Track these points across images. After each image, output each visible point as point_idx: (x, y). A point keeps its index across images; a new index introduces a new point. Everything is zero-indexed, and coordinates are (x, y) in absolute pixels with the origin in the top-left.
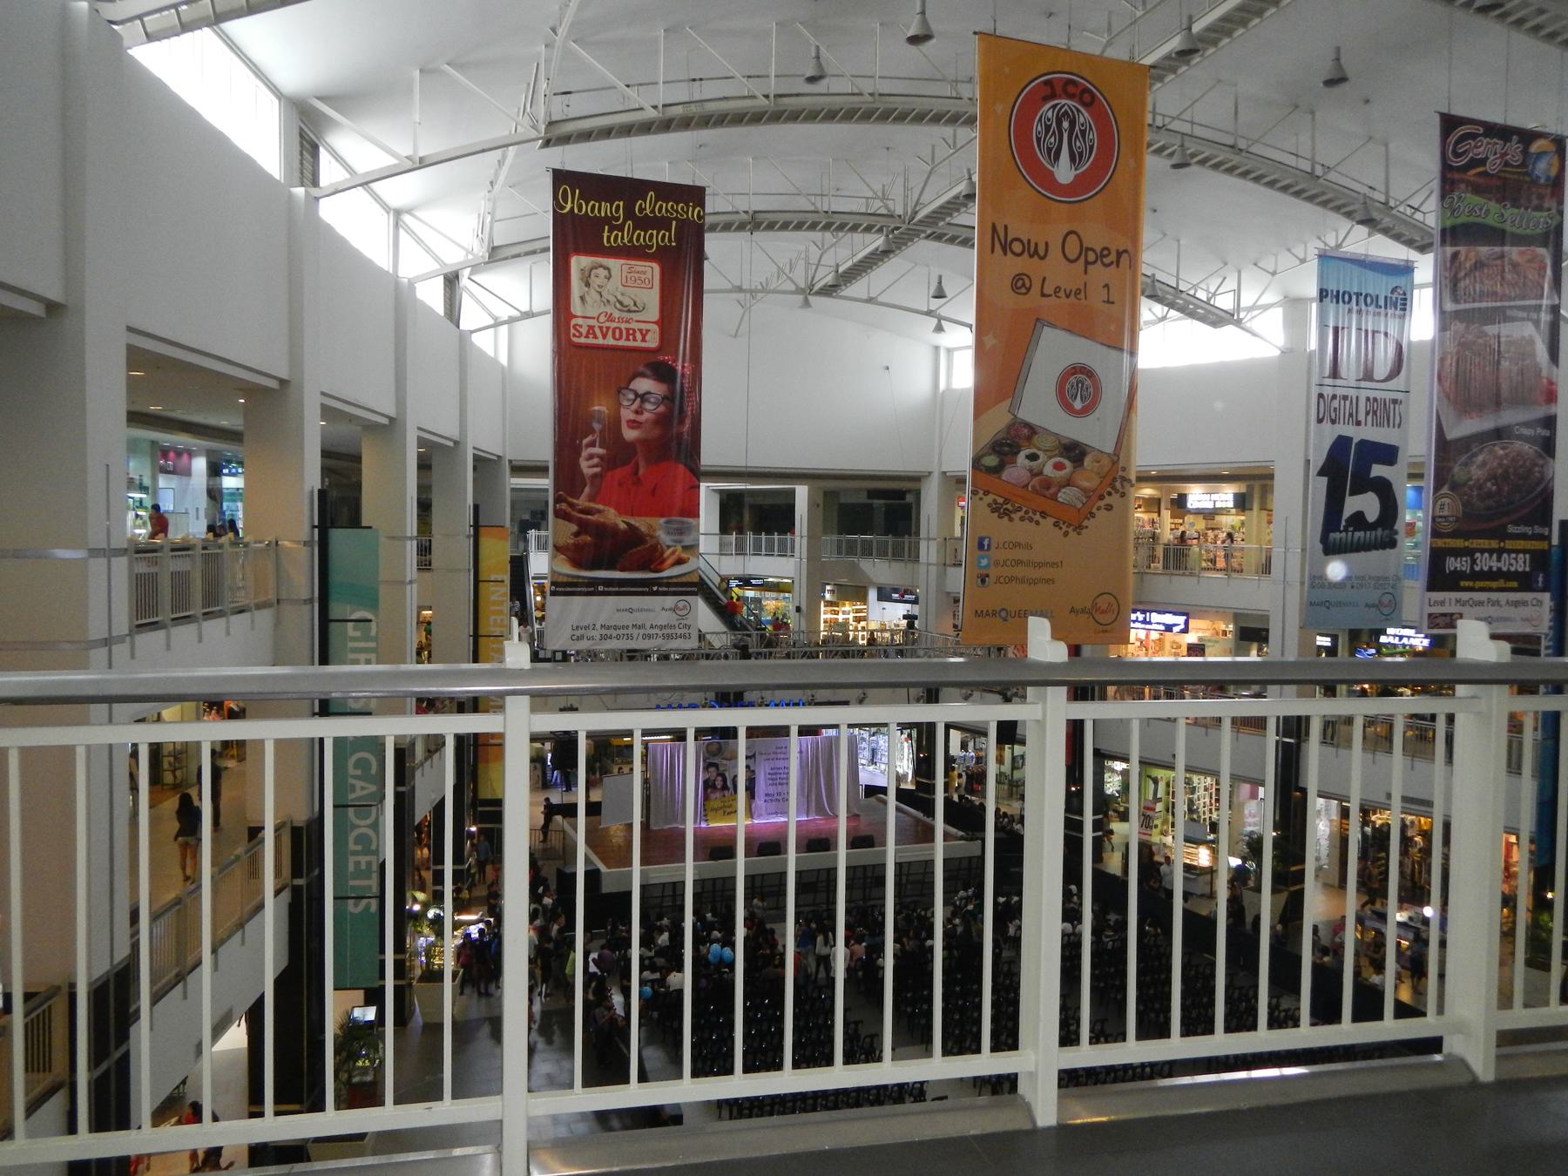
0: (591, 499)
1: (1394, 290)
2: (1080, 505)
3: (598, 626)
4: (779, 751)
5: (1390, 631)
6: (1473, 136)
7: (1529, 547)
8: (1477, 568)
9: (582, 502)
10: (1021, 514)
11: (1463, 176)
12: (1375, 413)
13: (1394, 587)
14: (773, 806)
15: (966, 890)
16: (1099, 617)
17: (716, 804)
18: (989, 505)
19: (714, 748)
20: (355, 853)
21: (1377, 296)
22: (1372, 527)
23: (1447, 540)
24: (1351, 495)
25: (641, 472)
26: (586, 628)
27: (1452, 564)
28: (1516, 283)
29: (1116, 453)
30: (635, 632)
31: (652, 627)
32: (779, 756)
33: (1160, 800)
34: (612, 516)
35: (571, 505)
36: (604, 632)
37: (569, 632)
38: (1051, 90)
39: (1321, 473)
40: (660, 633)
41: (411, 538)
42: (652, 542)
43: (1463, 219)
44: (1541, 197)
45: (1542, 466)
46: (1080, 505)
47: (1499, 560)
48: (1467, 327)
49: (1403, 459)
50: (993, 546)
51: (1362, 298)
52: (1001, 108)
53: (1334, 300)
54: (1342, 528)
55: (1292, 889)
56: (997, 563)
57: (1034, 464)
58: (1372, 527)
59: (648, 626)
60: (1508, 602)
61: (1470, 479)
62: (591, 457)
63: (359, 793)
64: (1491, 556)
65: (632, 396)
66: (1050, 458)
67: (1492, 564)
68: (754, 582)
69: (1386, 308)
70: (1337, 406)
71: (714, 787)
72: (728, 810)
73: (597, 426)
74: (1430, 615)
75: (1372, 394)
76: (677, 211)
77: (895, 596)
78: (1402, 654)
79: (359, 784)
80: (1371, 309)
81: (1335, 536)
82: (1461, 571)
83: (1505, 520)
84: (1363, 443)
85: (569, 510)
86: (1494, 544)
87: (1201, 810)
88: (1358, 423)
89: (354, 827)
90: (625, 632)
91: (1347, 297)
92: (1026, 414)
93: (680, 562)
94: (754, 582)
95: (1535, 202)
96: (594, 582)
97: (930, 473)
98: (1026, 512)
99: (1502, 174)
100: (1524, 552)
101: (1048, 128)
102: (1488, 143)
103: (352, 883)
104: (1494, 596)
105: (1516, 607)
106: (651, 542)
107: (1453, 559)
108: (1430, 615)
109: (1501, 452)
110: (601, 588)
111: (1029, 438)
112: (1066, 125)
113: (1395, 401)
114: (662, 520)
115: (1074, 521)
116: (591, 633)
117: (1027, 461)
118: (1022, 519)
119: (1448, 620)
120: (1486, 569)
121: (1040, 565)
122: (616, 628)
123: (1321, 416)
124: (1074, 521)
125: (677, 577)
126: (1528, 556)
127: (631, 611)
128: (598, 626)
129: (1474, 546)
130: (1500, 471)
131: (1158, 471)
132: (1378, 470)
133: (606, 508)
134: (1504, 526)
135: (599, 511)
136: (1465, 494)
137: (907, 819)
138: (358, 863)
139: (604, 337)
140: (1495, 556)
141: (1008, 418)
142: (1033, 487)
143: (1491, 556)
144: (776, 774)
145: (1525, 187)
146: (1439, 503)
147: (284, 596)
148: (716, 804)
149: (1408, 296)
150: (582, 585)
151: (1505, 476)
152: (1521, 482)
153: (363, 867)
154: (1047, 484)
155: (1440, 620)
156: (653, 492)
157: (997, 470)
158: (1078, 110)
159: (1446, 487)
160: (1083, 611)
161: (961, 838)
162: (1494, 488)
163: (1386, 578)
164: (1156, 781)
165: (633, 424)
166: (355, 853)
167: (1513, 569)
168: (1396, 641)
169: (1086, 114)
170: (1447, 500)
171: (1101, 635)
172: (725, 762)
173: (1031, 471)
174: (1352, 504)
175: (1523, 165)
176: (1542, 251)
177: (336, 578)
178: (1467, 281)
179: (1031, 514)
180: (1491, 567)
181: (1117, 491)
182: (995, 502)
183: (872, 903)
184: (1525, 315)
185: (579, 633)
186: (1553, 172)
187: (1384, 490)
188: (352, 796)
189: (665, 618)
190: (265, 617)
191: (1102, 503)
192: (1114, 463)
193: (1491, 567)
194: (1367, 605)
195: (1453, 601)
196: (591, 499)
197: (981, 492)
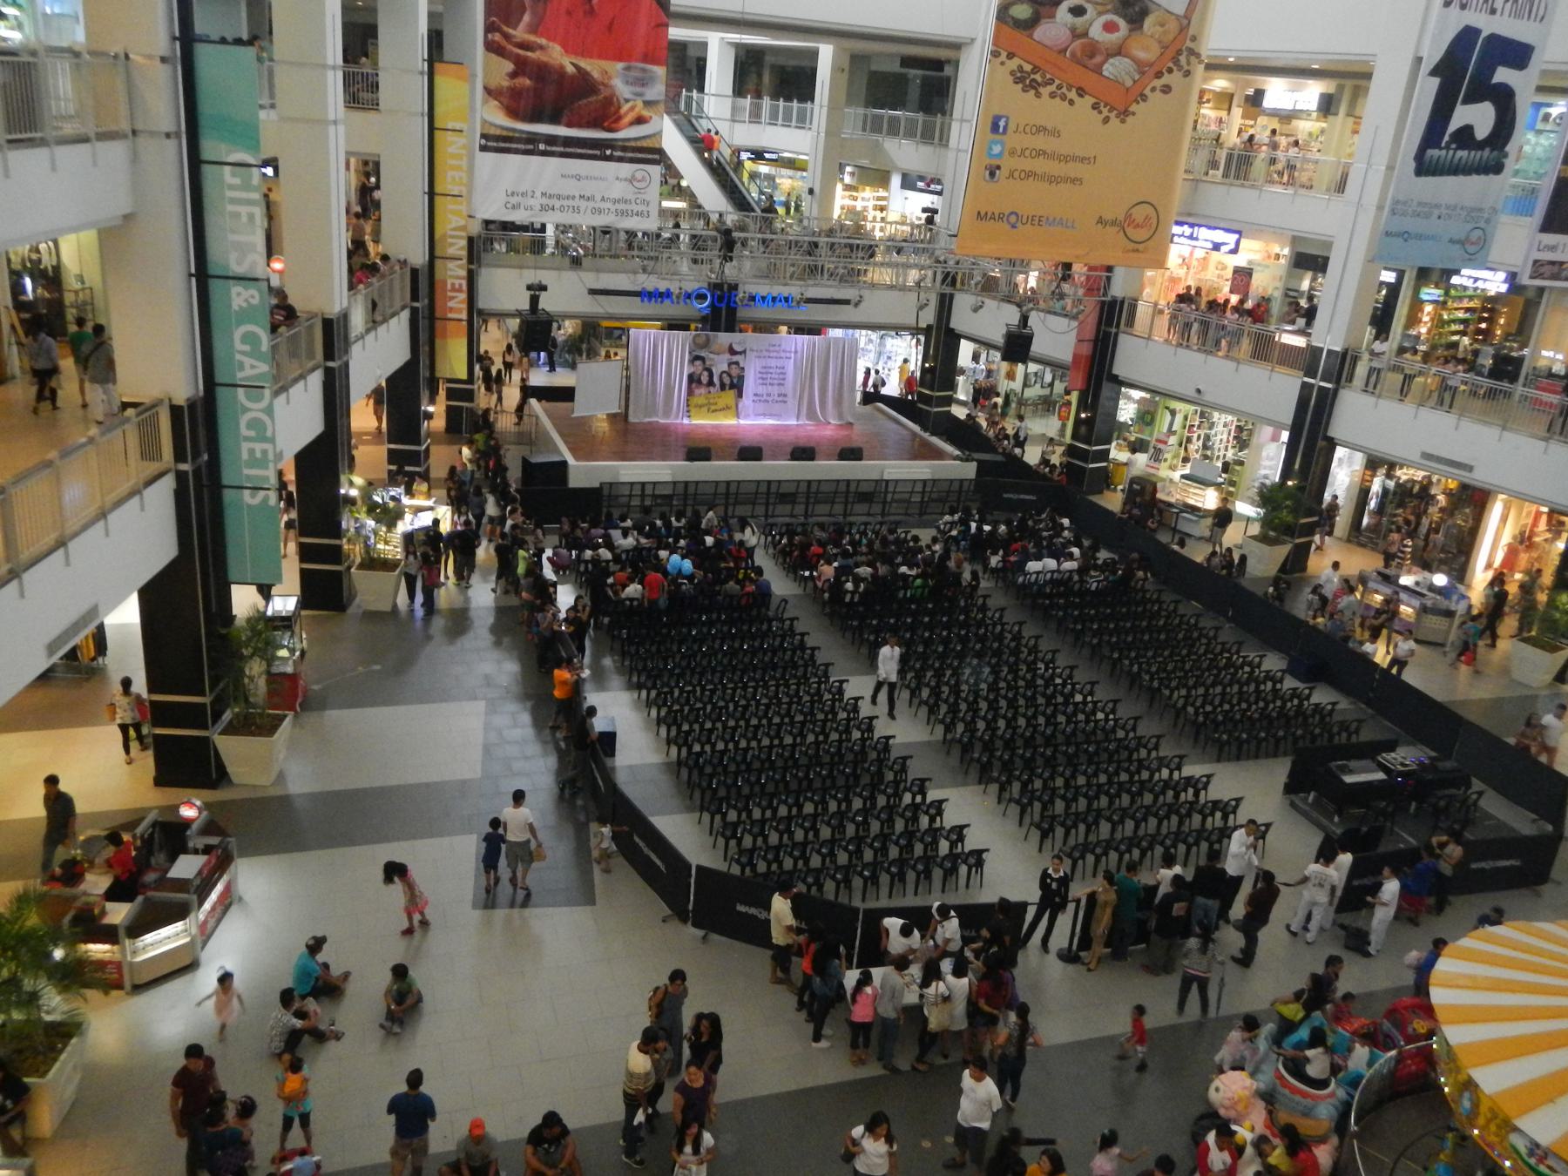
0: (533, 29)
2: (1129, 83)
3: (538, 194)
5: (1464, 272)
9: (520, 33)
10: (1053, 88)
13: (1488, 221)
14: (761, 407)
15: (952, 514)
16: (1133, 233)
17: (701, 401)
18: (1012, 73)
19: (701, 340)
20: (247, 439)
22: (1481, 145)
29: (1188, 16)
30: (583, 204)
31: (603, 199)
33: (1174, 433)
34: (557, 56)
35: (506, 36)
36: (545, 201)
37: (503, 198)
39: (1434, 72)
40: (613, 208)
41: (334, 68)
42: (604, 93)
46: (1129, 83)
49: (1537, 63)
50: (1012, 127)
55: (1298, 541)
56: (1012, 153)
57: (1079, 21)
58: (1481, 145)
59: (598, 198)
63: (248, 372)
66: (1100, 14)
68: (767, 156)
71: (699, 382)
74: (1536, 262)
77: (921, 184)
78: (1471, 298)
79: (247, 361)
81: (1433, 153)
84: (1494, 39)
85: (504, 43)
87: (1216, 446)
88: (1493, 11)
89: (246, 410)
93: (640, 120)
94: (767, 156)
96: (533, 139)
97: (973, 40)
98: (1060, 87)
103: (246, 471)
106: (604, 93)
108: (1536, 262)
110: (542, 147)
114: (620, 65)
116: (532, 202)
117: (1069, 18)
118: (1052, 95)
119: (1556, 269)
121: (1066, 159)
122: (559, 197)
125: (636, 139)
127: (578, 178)
128: (538, 194)
132: (1503, 75)
135: (541, 47)
137: (905, 432)
138: (252, 451)
142: (1073, 55)
147: (139, 126)
148: (701, 401)
150: (518, 140)
153: (258, 455)
154: (1092, 49)
155: (1547, 270)
156: (610, 27)
157: (1030, 24)
161: (956, 458)
163: (1480, 210)
164: (1173, 413)
166: (247, 439)
168: (1469, 283)
171: (1131, 255)
173: (1073, 30)
177: (206, 107)
179: (1064, 90)
181: (1180, 68)
182: (1020, 68)
183: (851, 519)
185: (514, 200)
187: (1504, 100)
188: (240, 375)
189: (618, 190)
190: (115, 152)
191: (1158, 83)
192: (1183, 29)
194: (1451, 241)
196: (533, 29)
197: (1004, 55)
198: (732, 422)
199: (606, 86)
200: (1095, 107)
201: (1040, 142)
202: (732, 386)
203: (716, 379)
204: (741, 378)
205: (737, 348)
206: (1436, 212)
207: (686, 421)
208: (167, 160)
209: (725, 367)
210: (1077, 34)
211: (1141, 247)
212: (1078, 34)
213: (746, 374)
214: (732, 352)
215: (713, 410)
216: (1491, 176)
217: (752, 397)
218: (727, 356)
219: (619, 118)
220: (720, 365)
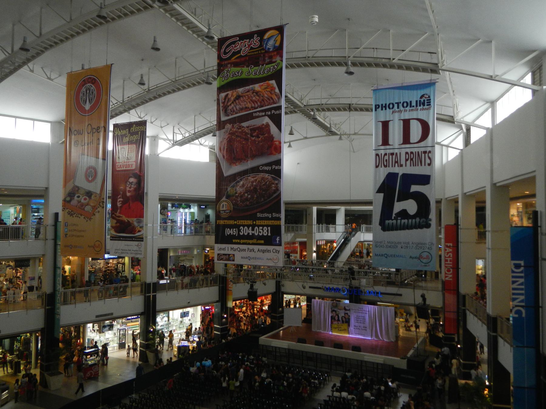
0: (120, 213)
1: (422, 97)
2: (91, 212)
4: (360, 309)
6: (234, 43)
8: (241, 234)
9: (118, 214)
10: (75, 215)
11: (230, 61)
12: (412, 159)
18: (68, 212)
19: (335, 304)
21: (411, 102)
23: (226, 221)
24: (398, 201)
25: (131, 205)
26: (118, 250)
27: (228, 232)
28: (258, 100)
30: (129, 252)
32: (359, 311)
34: (125, 219)
35: (116, 215)
38: (84, 82)
43: (230, 79)
44: (271, 57)
45: (277, 184)
47: (253, 230)
48: (233, 126)
50: (69, 225)
51: (401, 105)
52: (72, 93)
53: (384, 109)
54: (393, 218)
60: (259, 250)
61: (236, 193)
62: (120, 201)
65: (129, 183)
66: (83, 197)
67: (231, 232)
69: (417, 106)
70: (388, 159)
71: (335, 319)
72: (340, 329)
73: (121, 193)
74: (218, 254)
75: (409, 151)
76: (140, 129)
80: (408, 108)
83: (255, 211)
84: (404, 175)
86: (250, 222)
88: (401, 166)
90: (127, 251)
91: (391, 106)
92: (77, 184)
93: (139, 231)
95: (267, 60)
99: (249, 54)
101: (84, 94)
102: (241, 43)
104: (251, 247)
105: (263, 253)
107: (229, 229)
108: (218, 254)
111: (78, 191)
112: (88, 92)
113: (425, 152)
114: (136, 219)
115: (89, 217)
118: (76, 216)
120: (246, 234)
122: (124, 250)
123: (377, 164)
124: (89, 217)
125: (139, 236)
126: (269, 228)
127: (128, 245)
129: (240, 223)
130: (252, 188)
131: (178, 197)
132: (414, 188)
133: (123, 216)
134: (256, 214)
135: (121, 217)
136: (235, 200)
139: (123, 167)
140: (250, 228)
141: (72, 185)
144: (358, 318)
145: (262, 55)
146: (222, 204)
148: (336, 326)
149: (432, 98)
151: (255, 189)
154: (82, 205)
155: (224, 257)
158: (91, 86)
160: (416, 258)
162: (249, 196)
163: (425, 244)
165: (129, 191)
167: (261, 234)
169: (93, 86)
170: (224, 203)
172: (339, 310)
174: (398, 207)
175: (261, 45)
176: (273, 82)
178: (232, 105)
180: (249, 233)
184: (264, 114)
185: (116, 251)
186: (278, 44)
189: (135, 248)
192: (100, 197)
193: (249, 233)
195: (230, 249)
196: (120, 213)
198: (347, 335)
199: (133, 224)
200: (84, 218)
202: (346, 322)
203: (340, 319)
204: (349, 319)
205: (347, 308)
206: (399, 246)
208: (50, 244)
209: (343, 315)
211: (99, 253)
214: (345, 309)
215: (340, 330)
216: (419, 230)
218: (344, 311)
219: (136, 231)
220: (342, 314)
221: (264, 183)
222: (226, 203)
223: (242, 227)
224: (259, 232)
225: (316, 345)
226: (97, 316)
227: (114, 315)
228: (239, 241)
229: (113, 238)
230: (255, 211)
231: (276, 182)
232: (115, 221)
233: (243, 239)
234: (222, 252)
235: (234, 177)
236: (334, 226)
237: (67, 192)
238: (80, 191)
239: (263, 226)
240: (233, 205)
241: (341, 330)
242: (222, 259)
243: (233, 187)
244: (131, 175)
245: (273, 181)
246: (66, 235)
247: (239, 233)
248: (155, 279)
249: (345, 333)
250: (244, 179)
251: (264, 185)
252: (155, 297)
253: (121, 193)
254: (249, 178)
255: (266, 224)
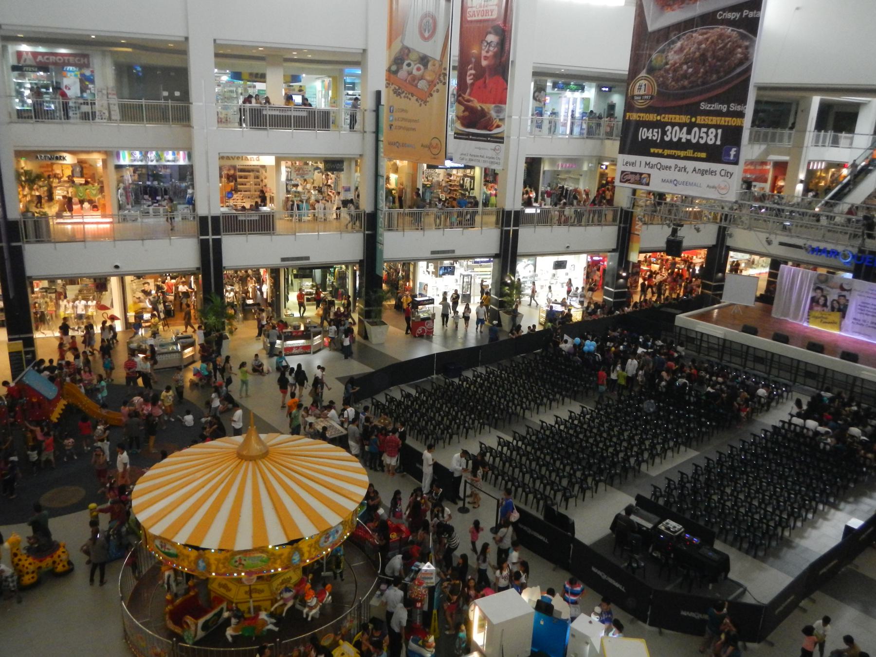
0: (470, 95)
7: (723, 123)
8: (667, 139)
9: (466, 96)
19: (823, 278)
23: (642, 115)
27: (645, 134)
30: (481, 159)
34: (477, 105)
35: (463, 98)
45: (747, 48)
60: (695, 170)
61: (667, 63)
62: (471, 75)
64: (681, 130)
71: (818, 303)
73: (473, 60)
74: (623, 172)
82: (652, 139)
83: (697, 99)
86: (685, 119)
93: (498, 126)
96: (469, 134)
100: (717, 127)
104: (681, 163)
105: (703, 175)
107: (645, 129)
108: (623, 172)
109: (701, 37)
111: (408, 55)
114: (493, 106)
115: (423, 99)
121: (410, 121)
124: (423, 99)
126: (720, 131)
127: (480, 149)
129: (666, 120)
130: (697, 54)
134: (698, 103)
136: (663, 77)
140: (685, 129)
143: (681, 130)
148: (817, 314)
151: (703, 57)
152: (719, 63)
157: (396, 72)
159: (645, 71)
165: (486, 58)
167: (702, 142)
170: (643, 82)
172: (828, 289)
180: (680, 139)
189: (491, 153)
192: (441, 65)
193: (680, 139)
195: (643, 164)
196: (470, 95)
198: (836, 332)
201: (404, 115)
202: (839, 310)
203: (829, 303)
204: (846, 306)
205: (846, 287)
207: (805, 324)
208: (370, 138)
210: (410, 73)
212: (410, 73)
213: (850, 304)
214: (842, 288)
215: (824, 322)
217: (851, 320)
218: (838, 291)
220: (833, 295)
221: (721, 46)
222: (646, 82)
223: (669, 128)
224: (700, 137)
225: (774, 339)
226: (433, 253)
227: (457, 254)
228: (660, 151)
229: (459, 136)
230: (697, 99)
231: (747, 43)
232: (462, 108)
233: (668, 149)
234: (630, 169)
235: (666, 34)
236: (851, 135)
237: (393, 57)
238: (410, 55)
239: (709, 127)
240: (658, 85)
241: (825, 323)
242: (628, 181)
243: (663, 51)
244: (490, 29)
245: (740, 42)
246: (391, 126)
247: (662, 138)
248: (518, 206)
249: (832, 328)
250: (684, 37)
251: (721, 49)
252: (516, 233)
253: (473, 60)
254: (694, 35)
255: (714, 122)
